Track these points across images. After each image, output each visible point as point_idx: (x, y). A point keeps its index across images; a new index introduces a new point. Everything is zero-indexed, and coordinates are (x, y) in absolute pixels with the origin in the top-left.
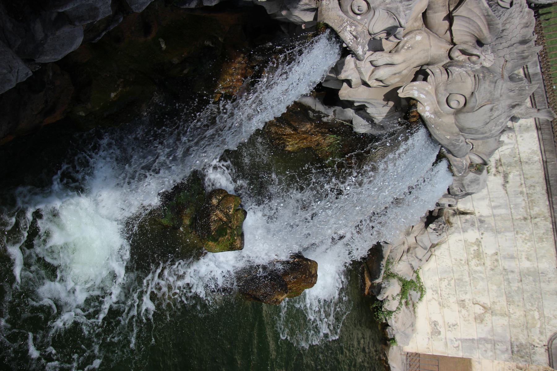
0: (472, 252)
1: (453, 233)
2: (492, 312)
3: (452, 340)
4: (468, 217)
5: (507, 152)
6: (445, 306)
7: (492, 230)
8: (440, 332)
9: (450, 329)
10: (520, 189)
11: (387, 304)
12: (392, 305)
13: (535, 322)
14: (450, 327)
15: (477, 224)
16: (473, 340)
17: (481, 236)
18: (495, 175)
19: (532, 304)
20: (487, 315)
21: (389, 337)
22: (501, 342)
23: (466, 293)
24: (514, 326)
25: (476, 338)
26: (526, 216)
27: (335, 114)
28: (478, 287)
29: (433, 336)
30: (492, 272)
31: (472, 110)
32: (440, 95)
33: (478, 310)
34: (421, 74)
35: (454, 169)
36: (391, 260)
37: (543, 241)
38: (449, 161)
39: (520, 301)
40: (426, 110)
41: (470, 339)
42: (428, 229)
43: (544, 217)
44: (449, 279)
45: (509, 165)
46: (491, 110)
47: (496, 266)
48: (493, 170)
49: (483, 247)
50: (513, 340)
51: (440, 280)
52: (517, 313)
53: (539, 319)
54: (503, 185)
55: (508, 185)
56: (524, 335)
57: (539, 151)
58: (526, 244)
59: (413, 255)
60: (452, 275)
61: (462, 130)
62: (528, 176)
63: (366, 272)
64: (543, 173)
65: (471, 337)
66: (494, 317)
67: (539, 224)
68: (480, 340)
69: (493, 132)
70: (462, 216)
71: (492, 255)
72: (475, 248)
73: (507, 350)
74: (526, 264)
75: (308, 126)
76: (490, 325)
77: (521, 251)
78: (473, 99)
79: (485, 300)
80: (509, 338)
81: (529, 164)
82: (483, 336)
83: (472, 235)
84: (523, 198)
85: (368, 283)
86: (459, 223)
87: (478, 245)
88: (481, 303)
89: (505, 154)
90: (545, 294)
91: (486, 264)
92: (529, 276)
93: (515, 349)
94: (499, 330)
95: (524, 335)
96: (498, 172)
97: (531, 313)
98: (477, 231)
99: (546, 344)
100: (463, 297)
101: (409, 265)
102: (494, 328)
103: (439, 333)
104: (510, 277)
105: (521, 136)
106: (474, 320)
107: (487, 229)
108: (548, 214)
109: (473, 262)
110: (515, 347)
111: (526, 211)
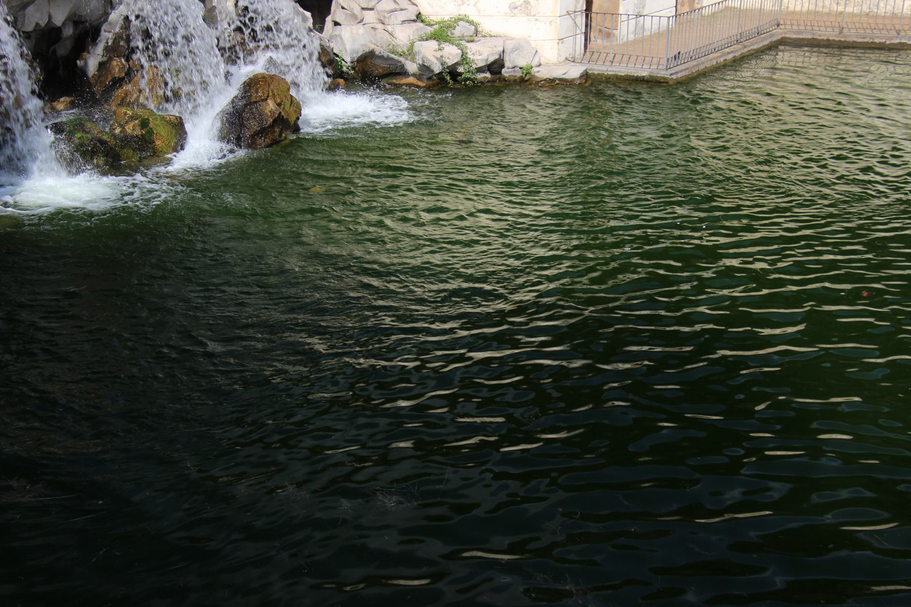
11: (447, 60)
12: (451, 54)
21: (519, 74)
27: (110, 32)
29: (533, 13)
36: (391, 47)
59: (387, 15)
63: (395, 81)
75: (114, 63)
85: (411, 80)
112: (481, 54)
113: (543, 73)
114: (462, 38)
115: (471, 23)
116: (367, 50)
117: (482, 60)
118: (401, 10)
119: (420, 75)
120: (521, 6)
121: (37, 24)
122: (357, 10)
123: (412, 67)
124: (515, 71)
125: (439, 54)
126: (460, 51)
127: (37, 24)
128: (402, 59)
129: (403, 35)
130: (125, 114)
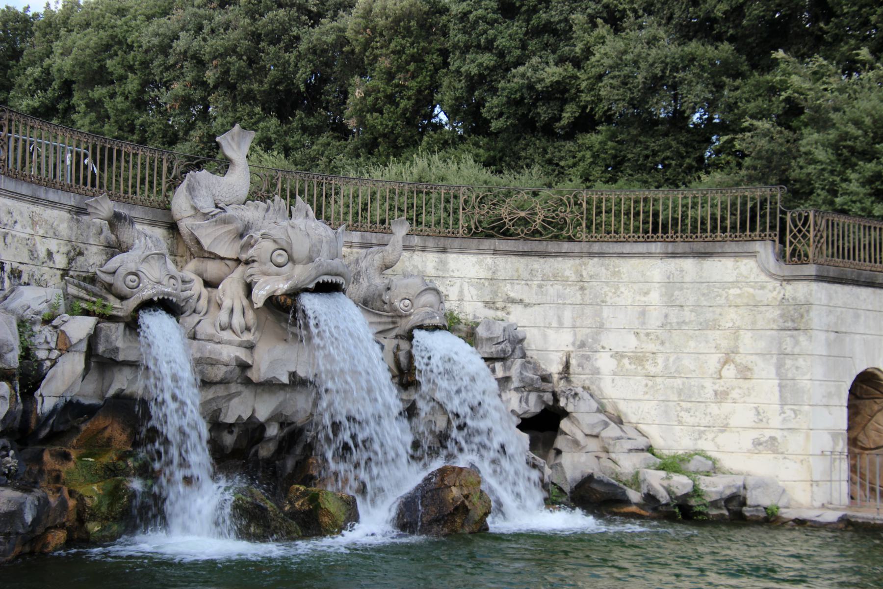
0: (633, 367)
1: (600, 389)
2: (733, 352)
3: (784, 420)
4: (573, 362)
5: (474, 291)
6: (725, 422)
7: (598, 334)
8: (771, 437)
9: (764, 420)
10: (535, 287)
12: (681, 483)
13: (746, 294)
14: (761, 420)
15: (586, 352)
16: (780, 386)
17: (607, 350)
18: (508, 313)
19: (717, 296)
20: (738, 359)
21: (762, 515)
22: (780, 343)
23: (702, 386)
24: (754, 323)
25: (777, 382)
26: (577, 288)
28: (692, 368)
30: (667, 345)
31: (291, 245)
32: (270, 271)
33: (730, 372)
34: (249, 289)
35: (427, 322)
37: (619, 271)
38: (421, 327)
39: (714, 312)
40: (282, 286)
41: (780, 391)
42: (569, 409)
43: (581, 265)
44: (679, 409)
45: (495, 293)
46: (293, 227)
47: (657, 337)
48: (500, 314)
49: (624, 350)
50: (775, 327)
51: (680, 423)
52: (731, 317)
53: (740, 289)
54: (526, 306)
55: (527, 301)
56: (767, 311)
57: (481, 257)
58: (622, 293)
59: (612, 442)
60: (671, 404)
61: (311, 260)
62: (516, 274)
63: (615, 510)
64: (513, 257)
65: (777, 389)
66: (741, 350)
67: (592, 273)
68: (780, 376)
69: (323, 234)
70: (571, 370)
71: (639, 339)
72: (626, 361)
73: (791, 336)
74: (655, 297)
76: (754, 357)
77: (634, 301)
78: (279, 241)
79: (713, 361)
80: (773, 332)
81: (497, 270)
82: (773, 370)
83: (604, 362)
84: (549, 287)
85: (633, 509)
86: (582, 376)
87: (623, 357)
88: (719, 366)
89: (477, 295)
90: (701, 277)
91: (654, 351)
92: (673, 295)
93: (790, 324)
94: (762, 345)
95: (767, 311)
96: (504, 309)
97: (731, 298)
98: (598, 355)
99: (779, 282)
100: (709, 393)
101: (633, 454)
102: (759, 352)
103: (773, 439)
104: (675, 320)
105: (453, 271)
106: (747, 381)
107: (596, 341)
108: (578, 261)
109: (651, 369)
110: (786, 324)
111: (569, 285)
112: (715, 487)
113: (789, 514)
114: (697, 472)
115: (709, 458)
116: (586, 475)
117: (717, 492)
118: (629, 439)
119: (644, 505)
120: (766, 442)
121: (240, 416)
122: (580, 436)
123: (634, 496)
124: (757, 510)
125: (665, 483)
126: (690, 481)
127: (240, 416)
128: (625, 488)
129: (627, 464)
130: (298, 489)
